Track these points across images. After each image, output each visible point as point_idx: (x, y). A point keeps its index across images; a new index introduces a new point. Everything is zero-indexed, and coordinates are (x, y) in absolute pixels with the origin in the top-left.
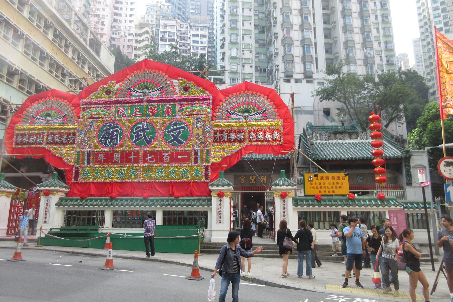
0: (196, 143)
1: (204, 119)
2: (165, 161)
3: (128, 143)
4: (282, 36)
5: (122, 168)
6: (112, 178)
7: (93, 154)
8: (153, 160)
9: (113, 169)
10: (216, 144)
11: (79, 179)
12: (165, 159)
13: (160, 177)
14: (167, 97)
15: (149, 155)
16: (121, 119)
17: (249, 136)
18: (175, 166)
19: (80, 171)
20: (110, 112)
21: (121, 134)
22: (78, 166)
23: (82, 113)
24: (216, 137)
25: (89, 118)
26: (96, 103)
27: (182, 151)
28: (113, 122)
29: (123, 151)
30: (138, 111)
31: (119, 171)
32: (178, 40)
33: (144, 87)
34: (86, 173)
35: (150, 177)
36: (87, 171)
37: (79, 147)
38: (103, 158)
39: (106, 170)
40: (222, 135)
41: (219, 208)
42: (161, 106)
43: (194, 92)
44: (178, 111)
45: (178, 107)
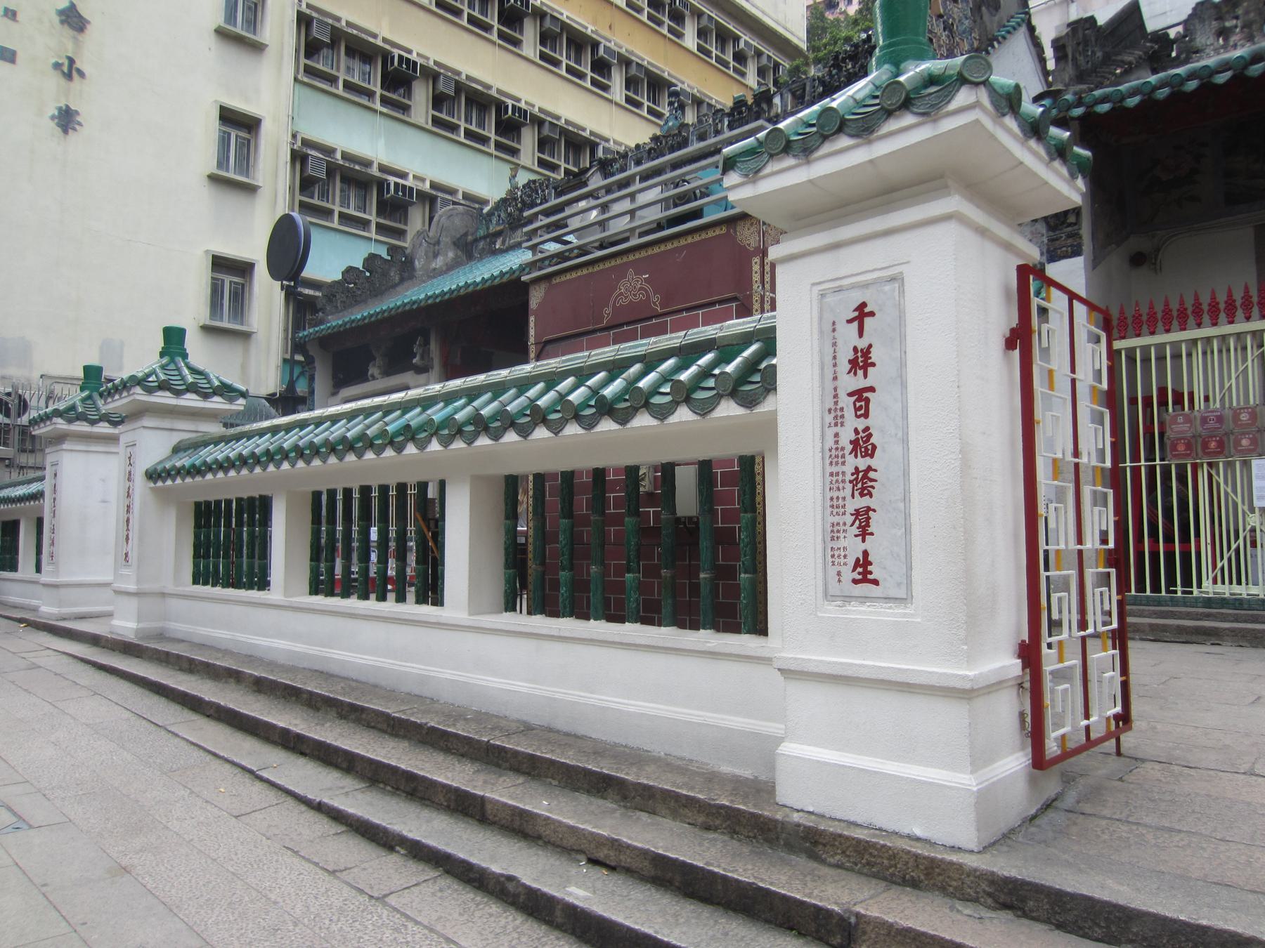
41: (847, 403)
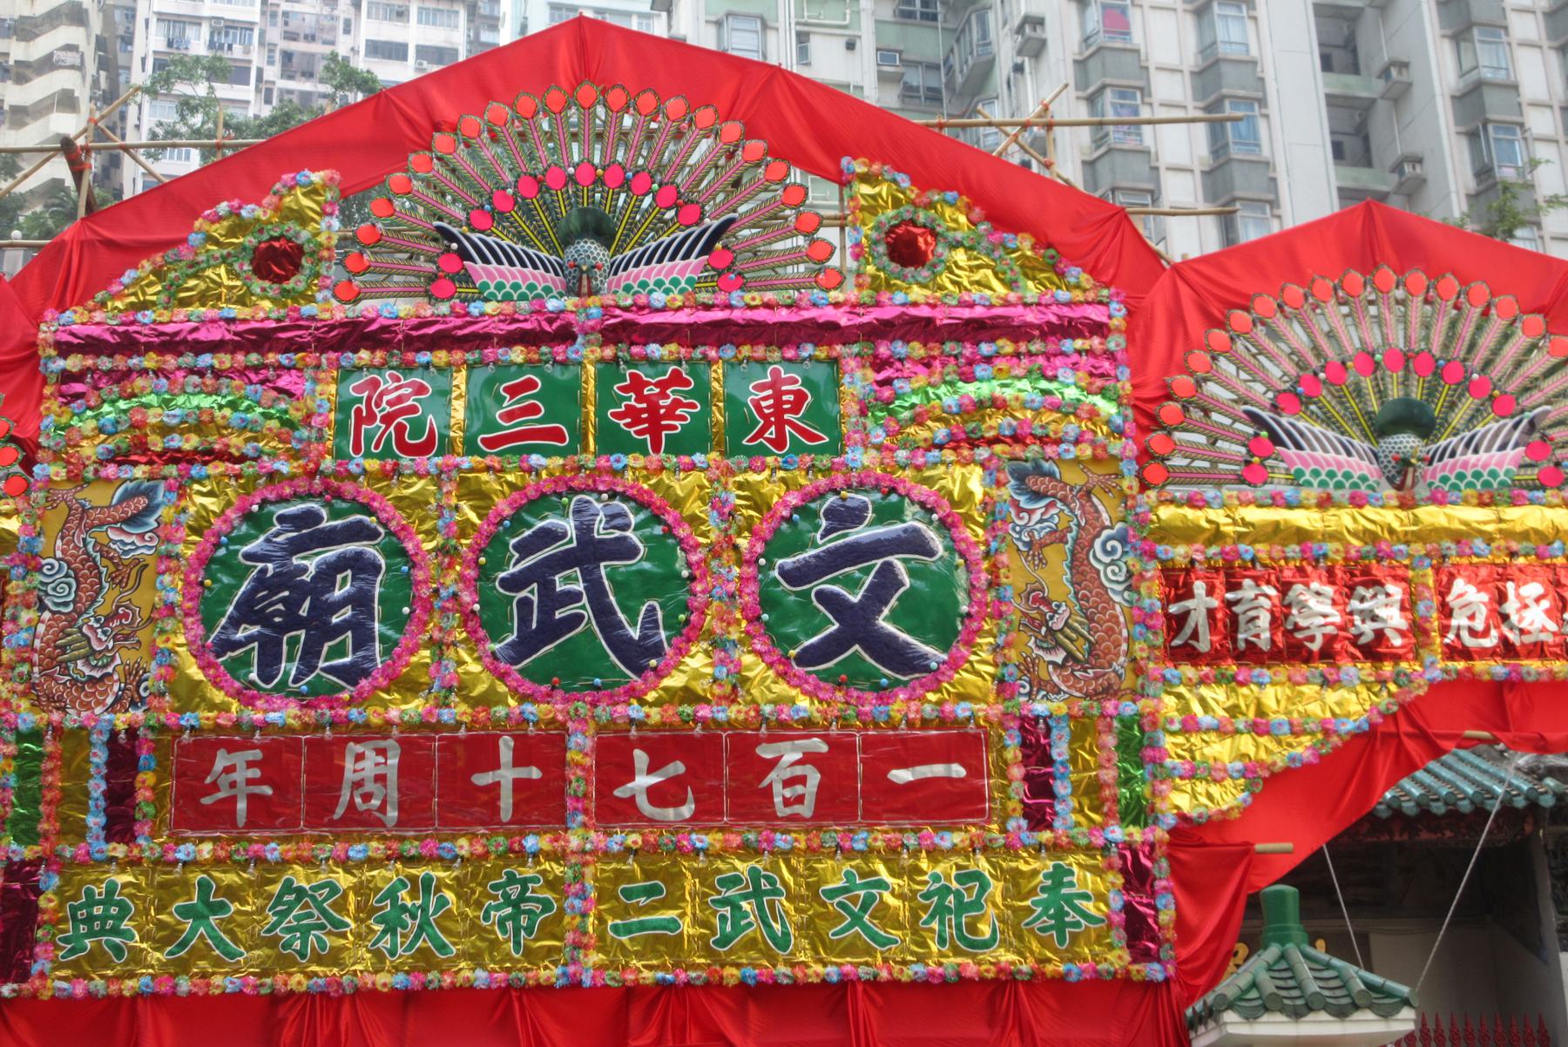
0: (1028, 666)
1: (1075, 478)
2: (782, 811)
3: (461, 663)
4: (1075, 37)
5: (420, 872)
6: (334, 957)
7: (156, 747)
8: (683, 802)
9: (344, 880)
10: (1188, 671)
11: (36, 968)
12: (780, 793)
13: (752, 943)
14: (768, 306)
15: (641, 757)
16: (396, 470)
17: (1446, 611)
18: (865, 855)
19: (42, 902)
20: (296, 416)
21: (403, 586)
22: (28, 852)
23: (52, 414)
24: (1183, 617)
25: (119, 458)
26: (171, 344)
27: (926, 723)
28: (327, 487)
29: (424, 725)
30: (533, 409)
31: (392, 894)
32: (272, 73)
33: (575, 223)
34: (104, 918)
35: (664, 942)
36: (108, 901)
37: (30, 689)
38: (250, 782)
39: (276, 889)
40: (1229, 604)
42: (718, 370)
43: (972, 269)
44: (863, 413)
45: (858, 382)
